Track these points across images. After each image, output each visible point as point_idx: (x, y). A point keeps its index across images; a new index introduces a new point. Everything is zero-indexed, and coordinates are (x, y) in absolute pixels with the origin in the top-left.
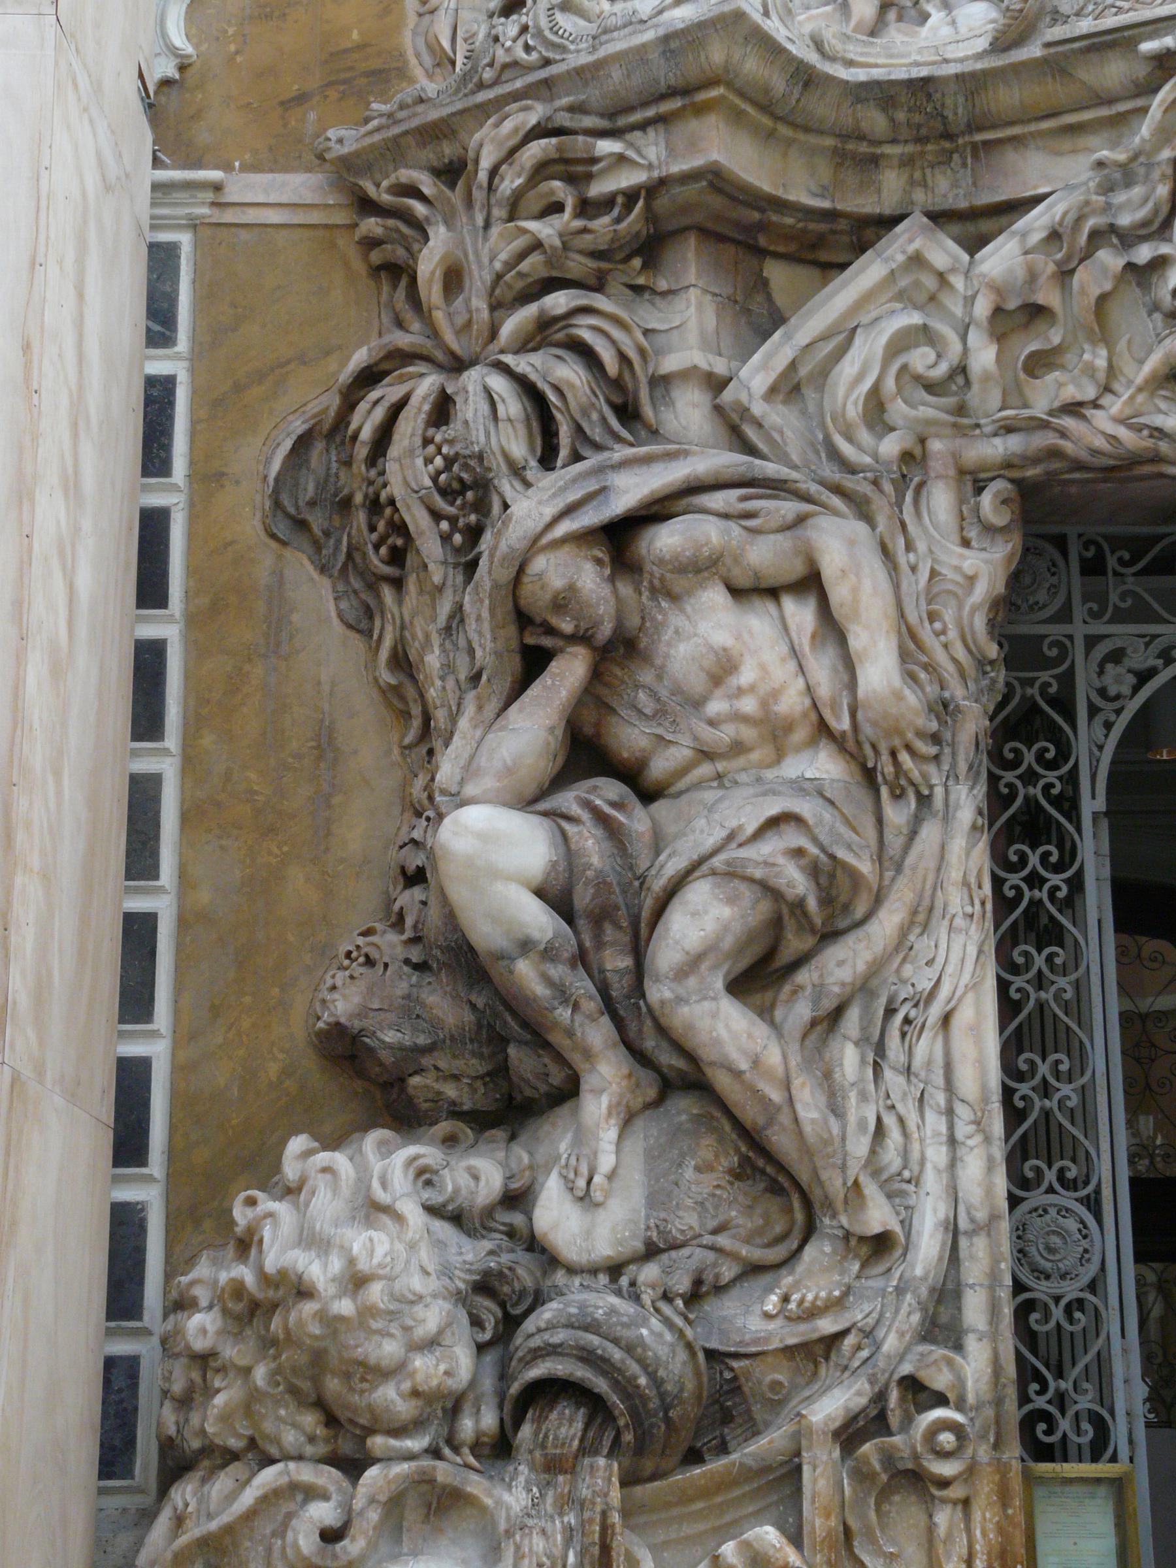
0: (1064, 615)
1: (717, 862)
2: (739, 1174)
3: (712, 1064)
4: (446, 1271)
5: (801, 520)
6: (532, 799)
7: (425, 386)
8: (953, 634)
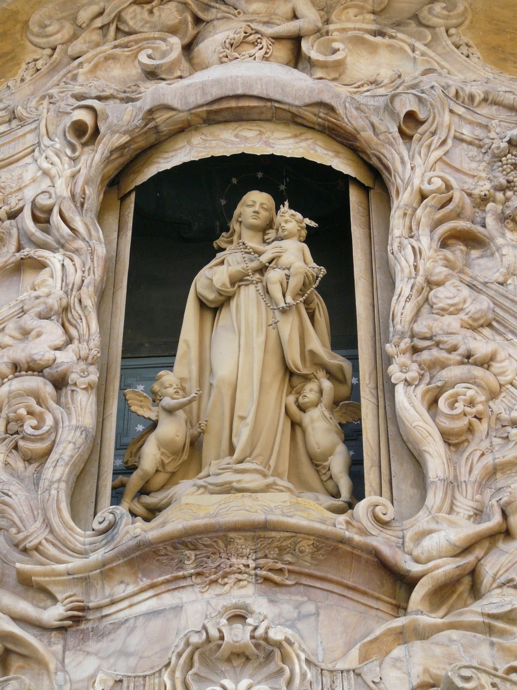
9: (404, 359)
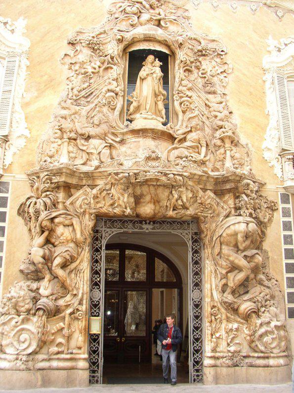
0: (102, 227)
1: (60, 255)
2: (61, 287)
4: (30, 296)
5: (71, 218)
6: (42, 247)
7: (34, 200)
8: (87, 231)
9: (176, 95)
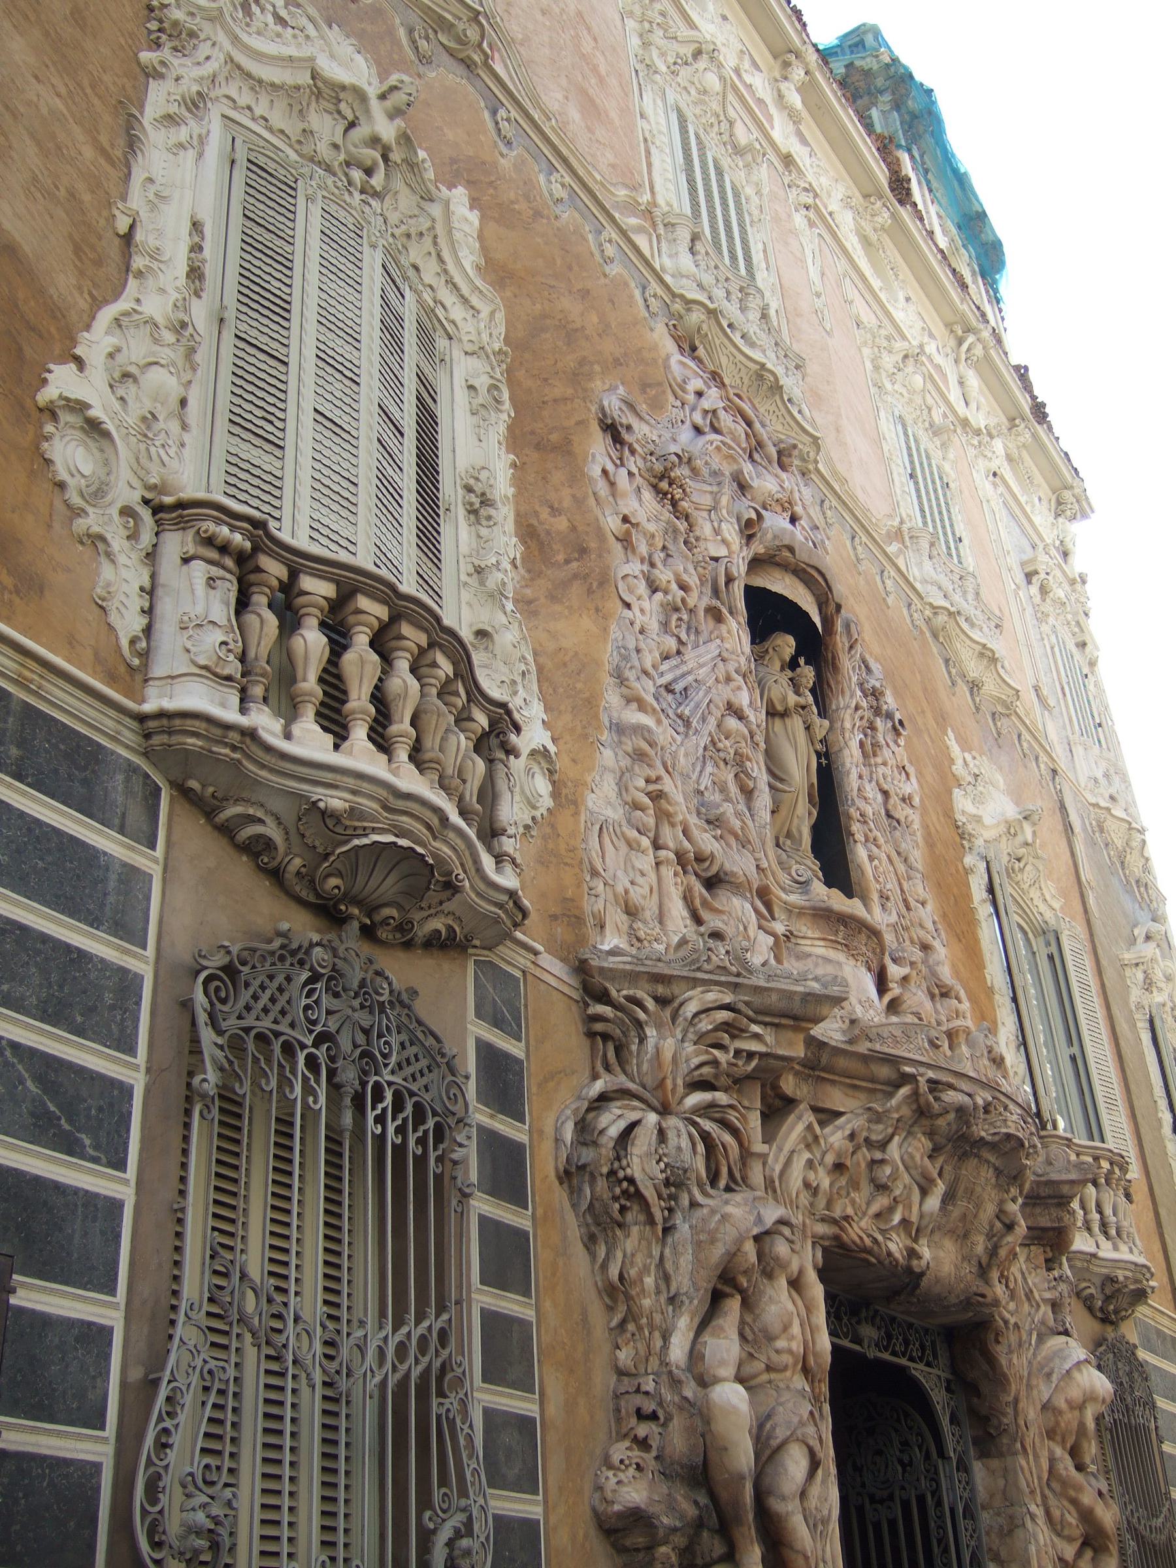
3: (798, 1552)
